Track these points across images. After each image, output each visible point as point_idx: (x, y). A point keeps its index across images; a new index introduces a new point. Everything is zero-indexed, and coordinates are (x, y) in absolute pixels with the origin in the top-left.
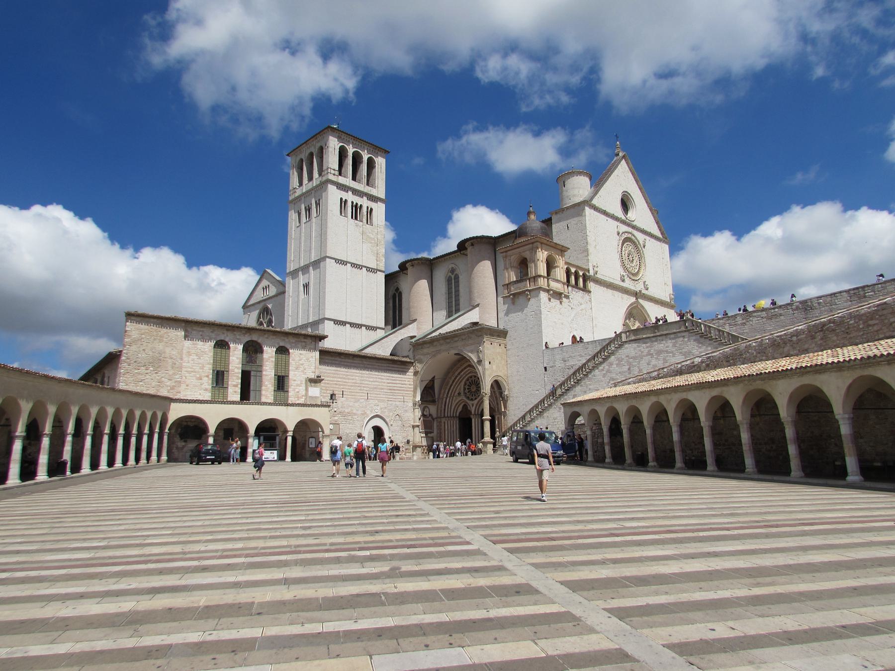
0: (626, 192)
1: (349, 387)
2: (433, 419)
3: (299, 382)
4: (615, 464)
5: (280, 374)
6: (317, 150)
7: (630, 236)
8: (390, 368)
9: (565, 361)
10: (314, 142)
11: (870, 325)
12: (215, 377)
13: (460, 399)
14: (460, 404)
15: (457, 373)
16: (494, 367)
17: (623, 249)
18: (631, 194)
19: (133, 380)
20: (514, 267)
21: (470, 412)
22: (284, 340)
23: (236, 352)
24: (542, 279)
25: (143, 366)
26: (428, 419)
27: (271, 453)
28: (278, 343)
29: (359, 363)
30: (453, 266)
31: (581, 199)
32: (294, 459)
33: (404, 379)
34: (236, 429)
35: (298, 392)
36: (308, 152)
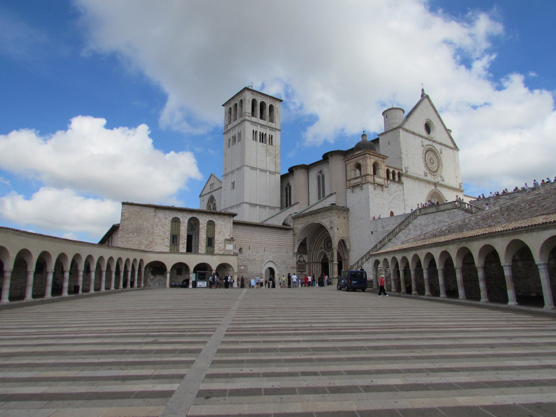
0: (429, 119)
1: (254, 244)
2: (306, 264)
3: (221, 242)
4: (397, 292)
5: (210, 237)
7: (431, 147)
8: (278, 233)
9: (384, 228)
10: (238, 97)
11: (532, 207)
12: (172, 239)
13: (321, 251)
14: (322, 254)
15: (319, 235)
16: (341, 232)
18: (432, 121)
19: (126, 241)
20: (353, 170)
21: (328, 259)
22: (212, 217)
23: (184, 224)
25: (131, 233)
27: (203, 283)
28: (208, 219)
29: (260, 230)
30: (321, 169)
31: (398, 125)
33: (287, 239)
34: (184, 269)
35: (220, 247)
36: (234, 103)
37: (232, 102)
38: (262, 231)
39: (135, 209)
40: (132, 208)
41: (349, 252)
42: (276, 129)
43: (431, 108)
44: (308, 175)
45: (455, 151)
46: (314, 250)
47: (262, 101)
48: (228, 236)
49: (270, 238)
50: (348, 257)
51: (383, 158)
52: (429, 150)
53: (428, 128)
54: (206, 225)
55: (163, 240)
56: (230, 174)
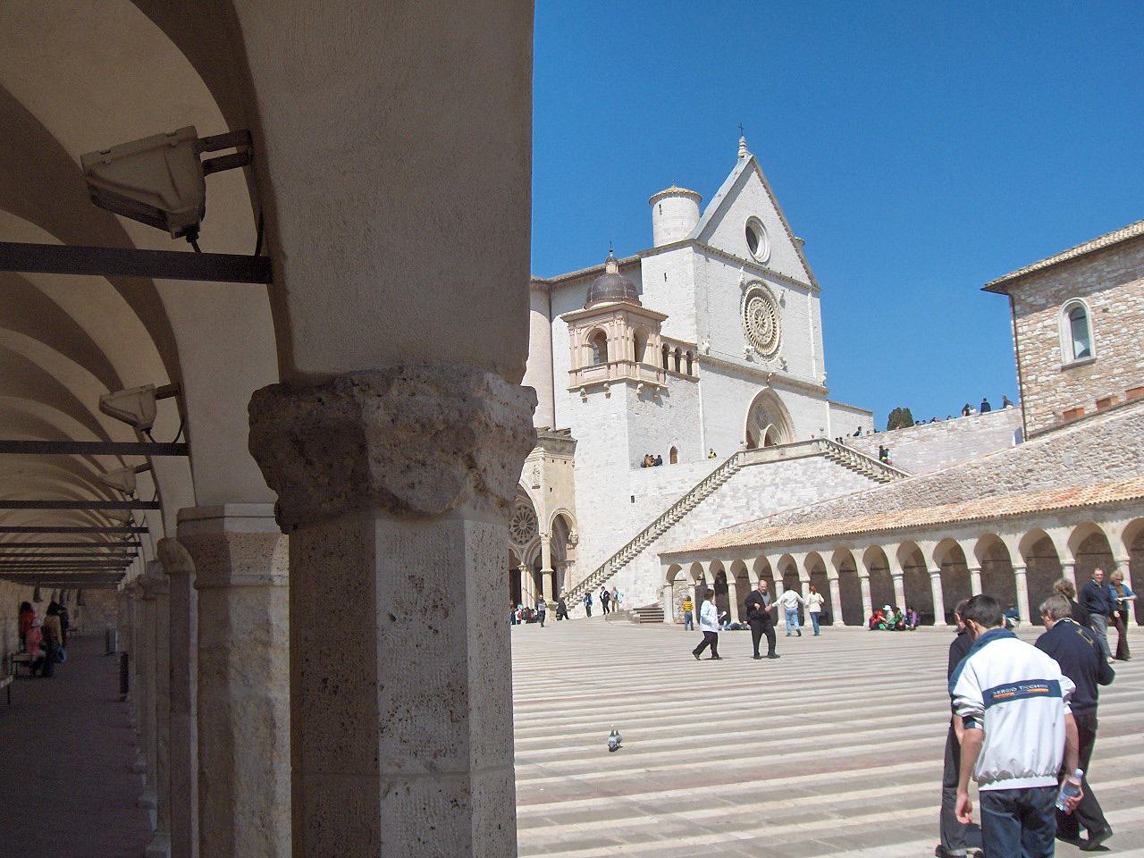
0: (754, 217)
7: (758, 286)
17: (749, 308)
52: (754, 294)
53: (752, 238)
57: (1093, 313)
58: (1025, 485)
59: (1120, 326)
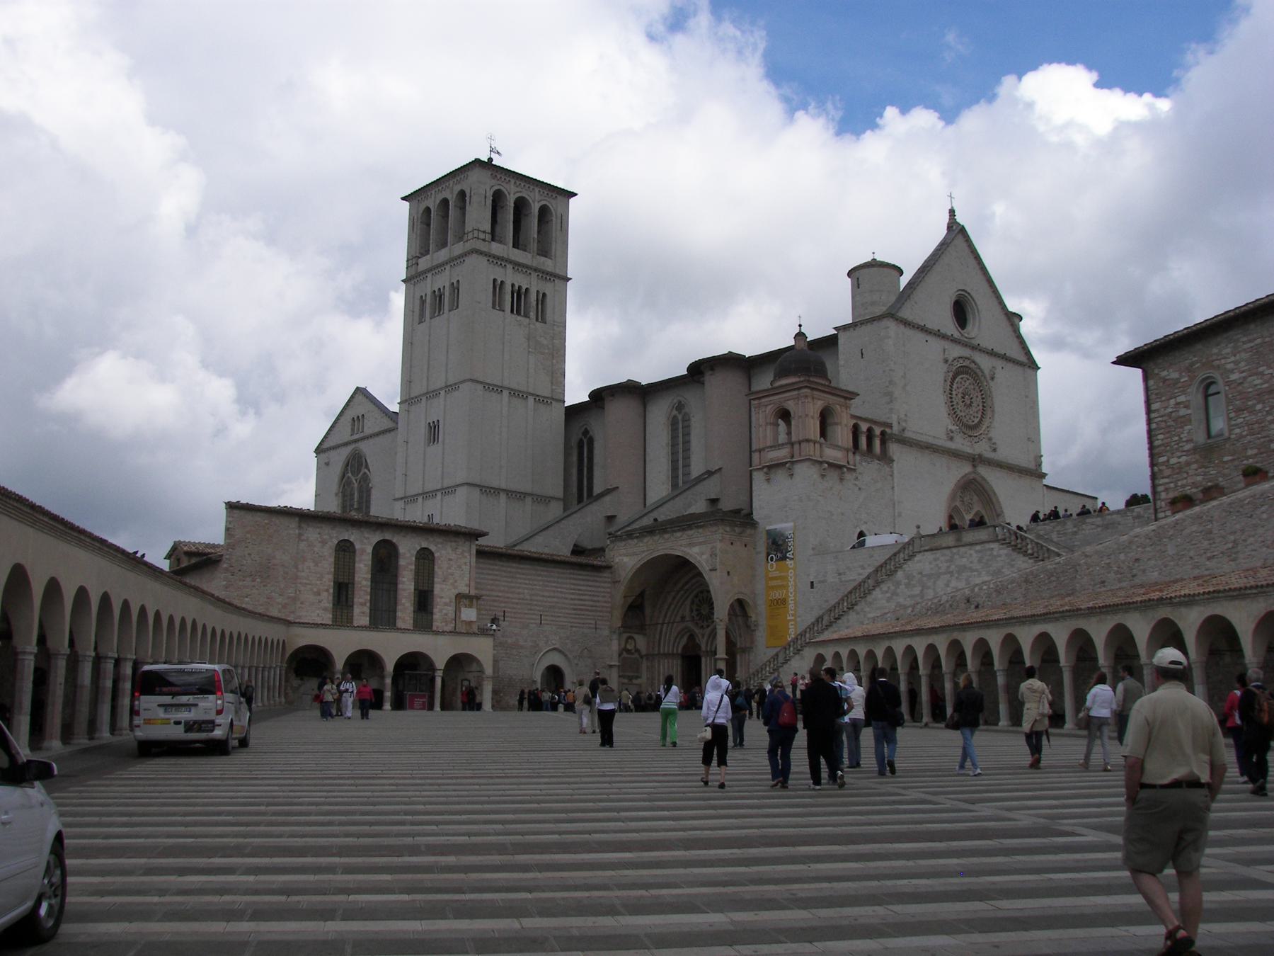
3: (448, 600)
5: (421, 588)
6: (455, 196)
7: (967, 363)
9: (840, 574)
10: (451, 182)
17: (955, 386)
18: (972, 294)
21: (699, 647)
24: (812, 444)
26: (633, 656)
30: (680, 398)
32: (443, 708)
35: (446, 614)
36: (440, 197)
37: (433, 192)
38: (534, 572)
39: (259, 519)
40: (249, 518)
41: (754, 630)
42: (555, 276)
43: (973, 262)
44: (645, 411)
45: (1029, 371)
46: (663, 624)
47: (519, 195)
48: (465, 588)
49: (554, 591)
50: (752, 642)
51: (846, 398)
53: (961, 311)
54: (414, 559)
55: (318, 594)
56: (424, 399)
57: (1227, 388)
58: (1133, 576)
59: (1255, 402)
